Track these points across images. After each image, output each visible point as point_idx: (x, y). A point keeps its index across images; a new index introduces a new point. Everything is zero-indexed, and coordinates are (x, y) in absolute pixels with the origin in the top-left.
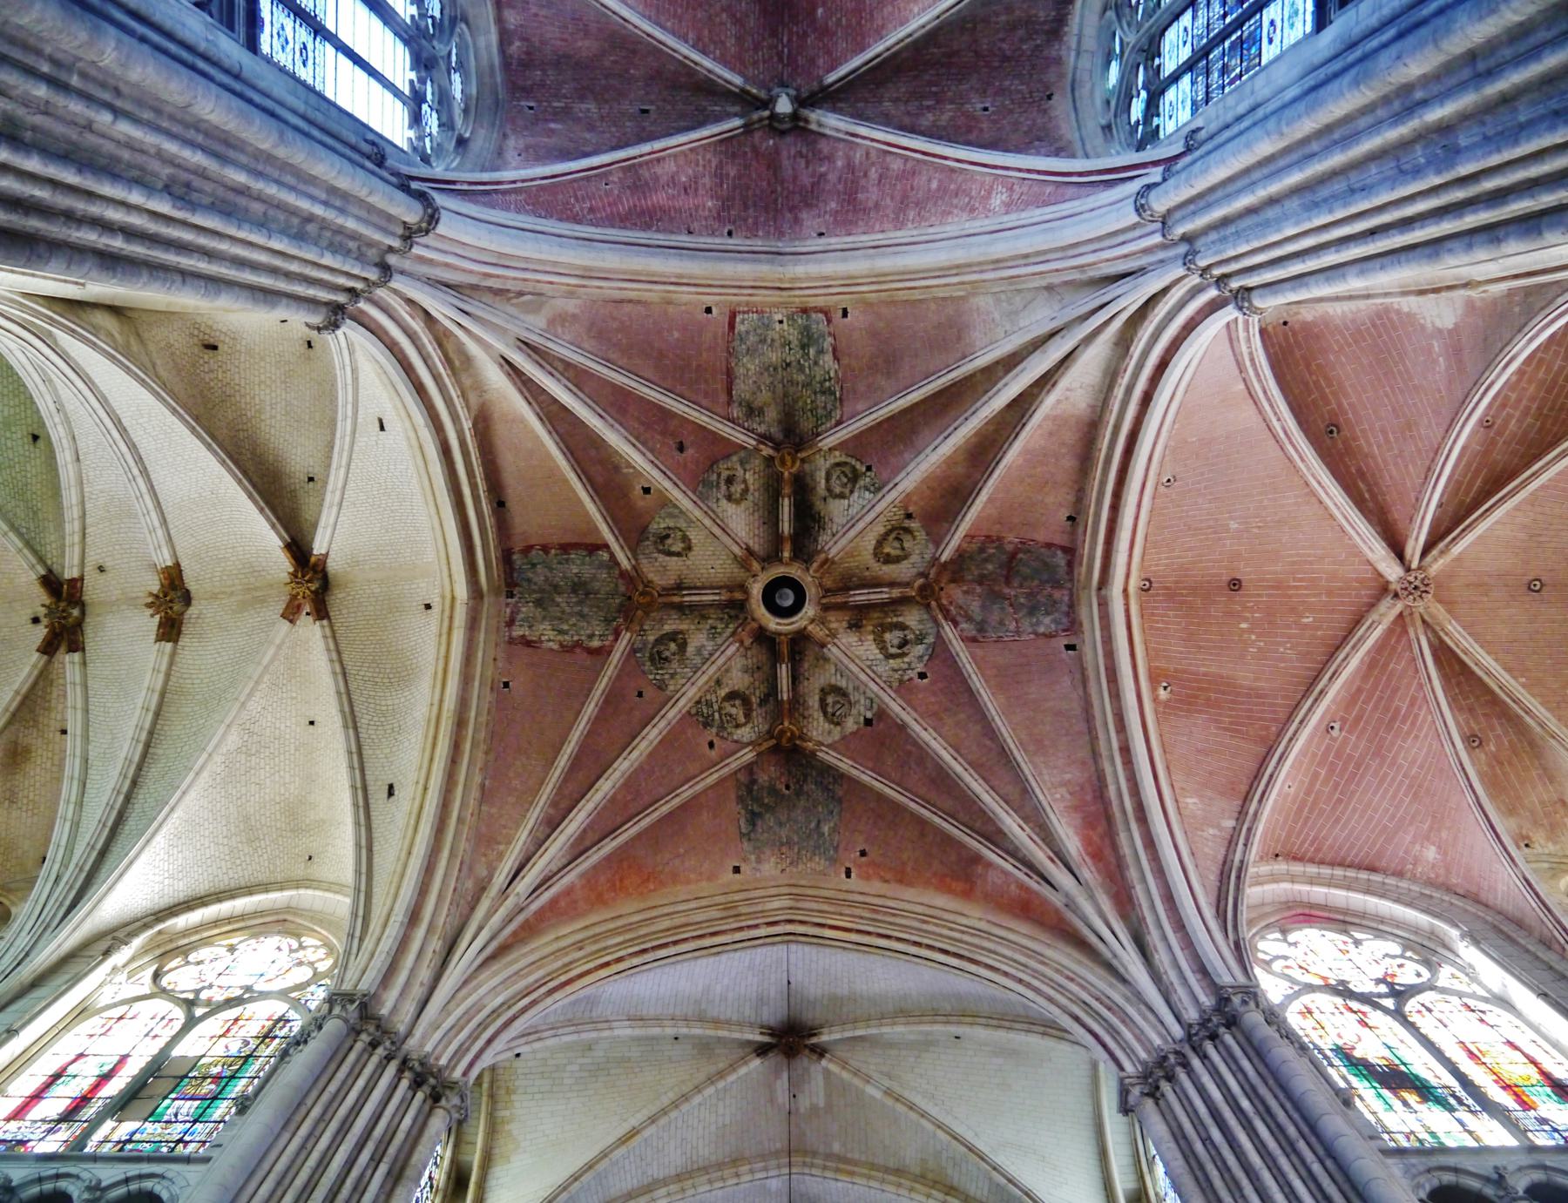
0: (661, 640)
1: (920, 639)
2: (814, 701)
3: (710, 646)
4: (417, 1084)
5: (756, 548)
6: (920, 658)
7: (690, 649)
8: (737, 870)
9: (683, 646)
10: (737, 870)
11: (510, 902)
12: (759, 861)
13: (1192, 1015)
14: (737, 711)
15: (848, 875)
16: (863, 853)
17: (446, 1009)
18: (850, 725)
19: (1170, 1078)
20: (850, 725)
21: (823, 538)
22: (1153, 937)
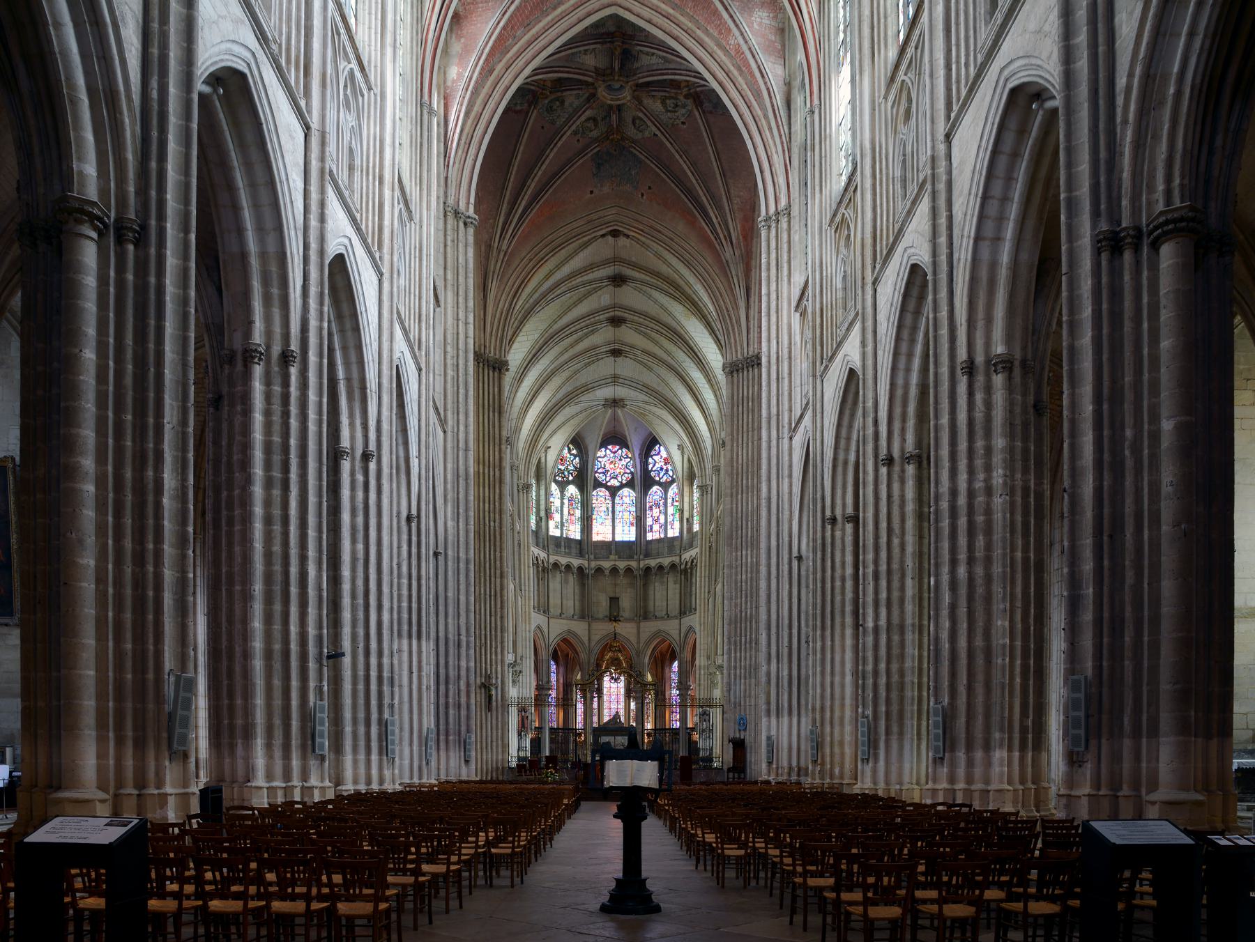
0: (551, 101)
1: (684, 106)
2: (629, 120)
3: (576, 103)
4: (494, 368)
5: (600, 65)
6: (683, 115)
7: (567, 104)
8: (592, 192)
9: (562, 103)
10: (592, 192)
11: (502, 254)
12: (602, 186)
13: (750, 353)
14: (591, 124)
15: (642, 195)
16: (650, 188)
17: (492, 324)
18: (647, 134)
19: (737, 371)
20: (647, 134)
21: (636, 65)
22: (752, 300)
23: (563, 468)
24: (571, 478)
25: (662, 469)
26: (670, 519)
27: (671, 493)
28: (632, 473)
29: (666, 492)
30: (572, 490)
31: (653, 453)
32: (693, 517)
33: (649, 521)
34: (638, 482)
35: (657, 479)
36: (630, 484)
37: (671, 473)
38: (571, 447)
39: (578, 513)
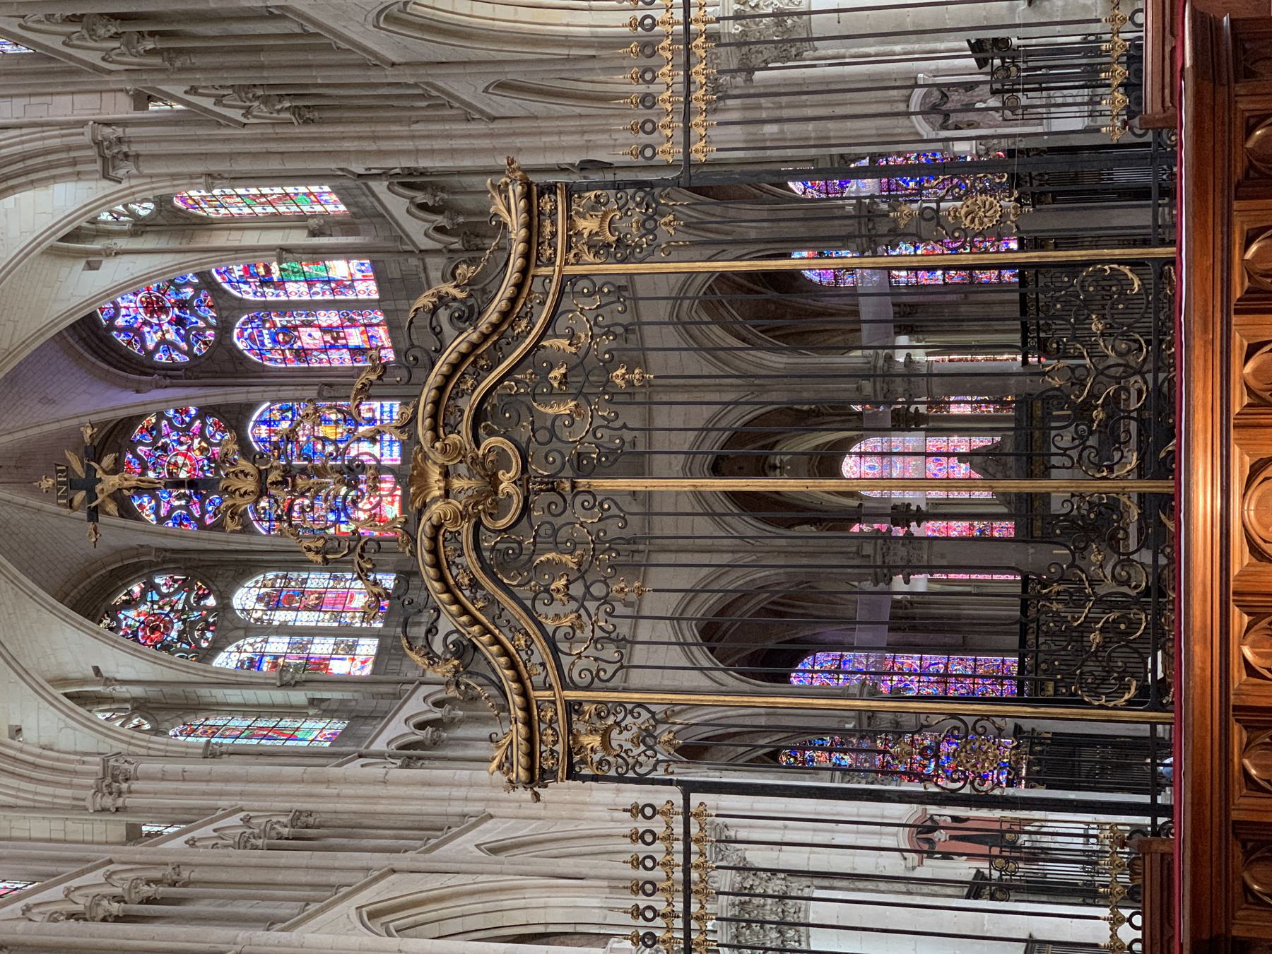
23: (178, 626)
24: (211, 602)
25: (179, 322)
26: (322, 294)
27: (248, 293)
28: (204, 412)
29: (243, 305)
30: (245, 598)
31: (136, 349)
32: (303, 217)
33: (339, 359)
34: (216, 396)
35: (210, 335)
36: (234, 417)
37: (188, 292)
38: (122, 597)
39: (317, 581)
